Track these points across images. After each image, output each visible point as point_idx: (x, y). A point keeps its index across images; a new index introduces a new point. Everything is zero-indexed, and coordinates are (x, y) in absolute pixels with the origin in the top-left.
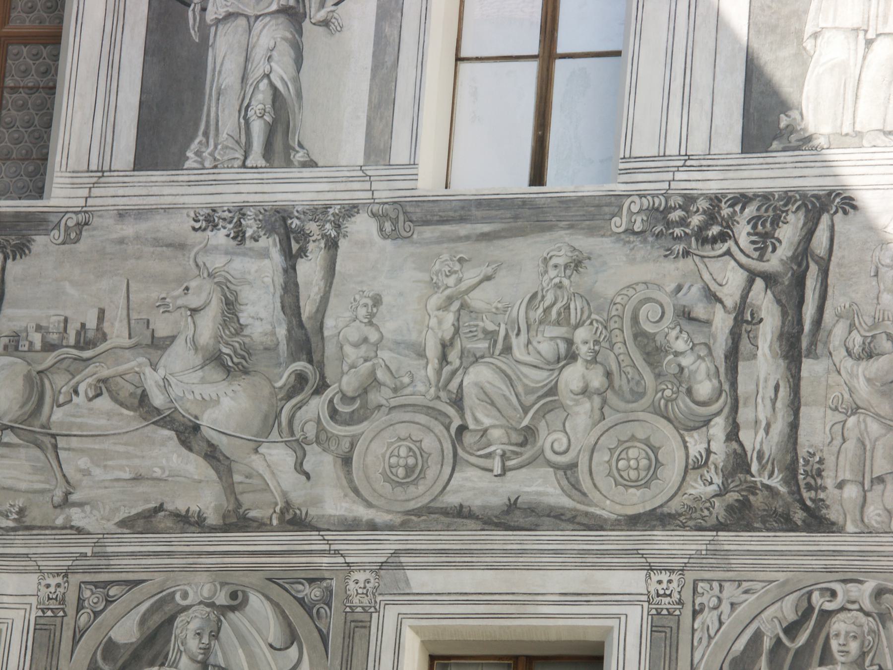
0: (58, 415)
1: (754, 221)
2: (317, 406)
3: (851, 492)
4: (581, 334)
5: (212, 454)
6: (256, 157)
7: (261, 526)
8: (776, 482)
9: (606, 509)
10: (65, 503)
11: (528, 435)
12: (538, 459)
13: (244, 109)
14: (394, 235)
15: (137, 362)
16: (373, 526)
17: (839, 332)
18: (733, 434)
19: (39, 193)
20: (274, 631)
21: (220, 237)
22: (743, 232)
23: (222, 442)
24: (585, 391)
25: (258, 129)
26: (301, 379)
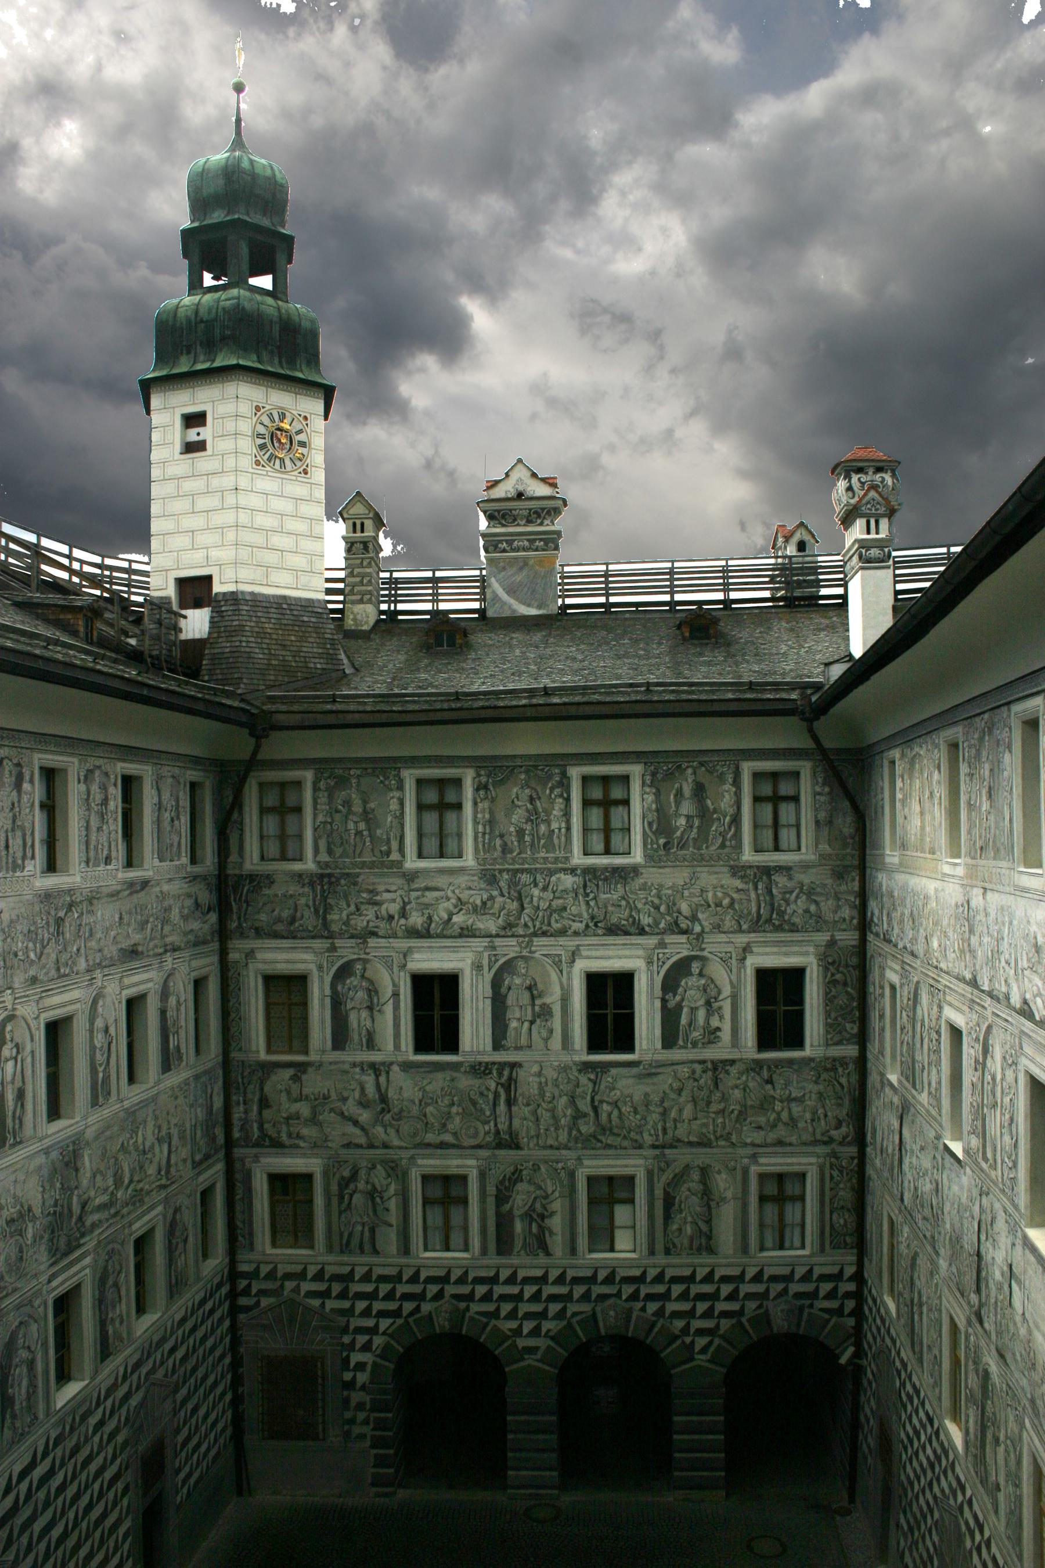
0: (321, 1117)
1: (497, 1069)
2: (388, 1117)
3: (525, 1140)
4: (455, 1099)
5: (363, 1129)
6: (364, 1048)
7: (377, 1147)
8: (507, 1137)
9: (465, 1144)
10: (326, 1140)
11: (444, 1125)
12: (447, 1131)
13: (360, 1035)
14: (404, 1071)
15: (339, 1104)
16: (406, 1148)
17: (520, 1099)
18: (496, 1125)
19: (306, 1052)
20: (383, 1173)
21: (357, 1070)
22: (495, 1072)
23: (366, 1126)
24: (458, 1113)
25: (364, 1040)
26: (383, 1110)
